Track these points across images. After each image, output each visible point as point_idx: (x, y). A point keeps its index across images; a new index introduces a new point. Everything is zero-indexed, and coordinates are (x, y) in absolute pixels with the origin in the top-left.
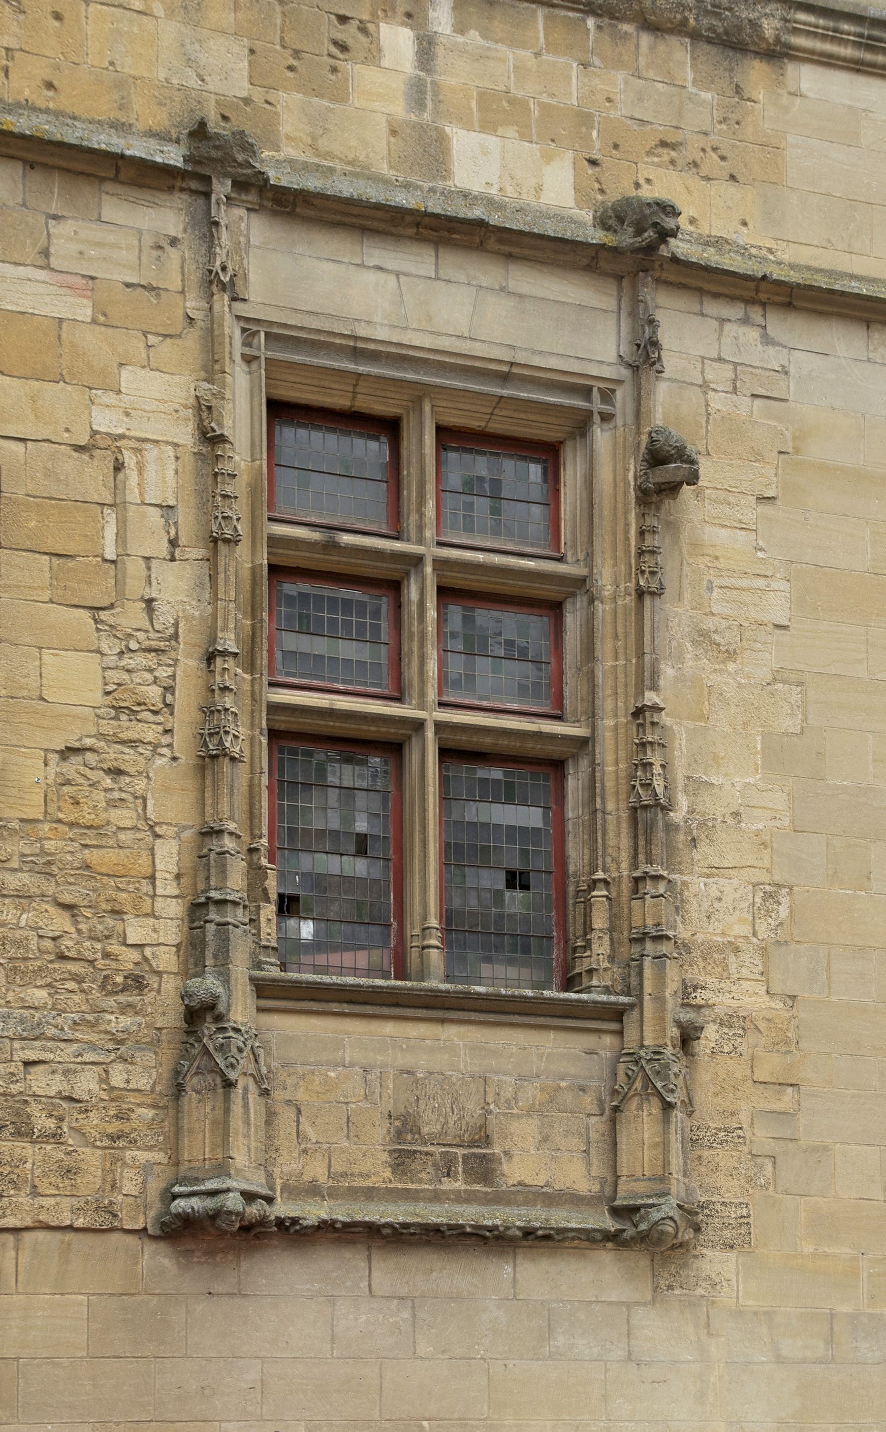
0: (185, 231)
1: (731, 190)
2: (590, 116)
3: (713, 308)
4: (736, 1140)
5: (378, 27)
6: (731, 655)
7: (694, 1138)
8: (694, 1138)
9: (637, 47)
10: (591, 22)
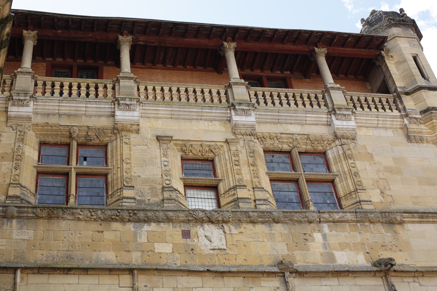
0: (280, 285)
1: (401, 253)
2: (364, 243)
3: (406, 280)
5: (313, 234)
9: (370, 227)
10: (359, 224)
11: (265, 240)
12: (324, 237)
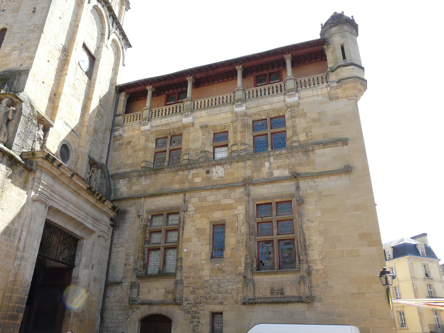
3: (307, 181)
6: (313, 222)
10: (289, 154)
11: (242, 170)
12: (270, 164)
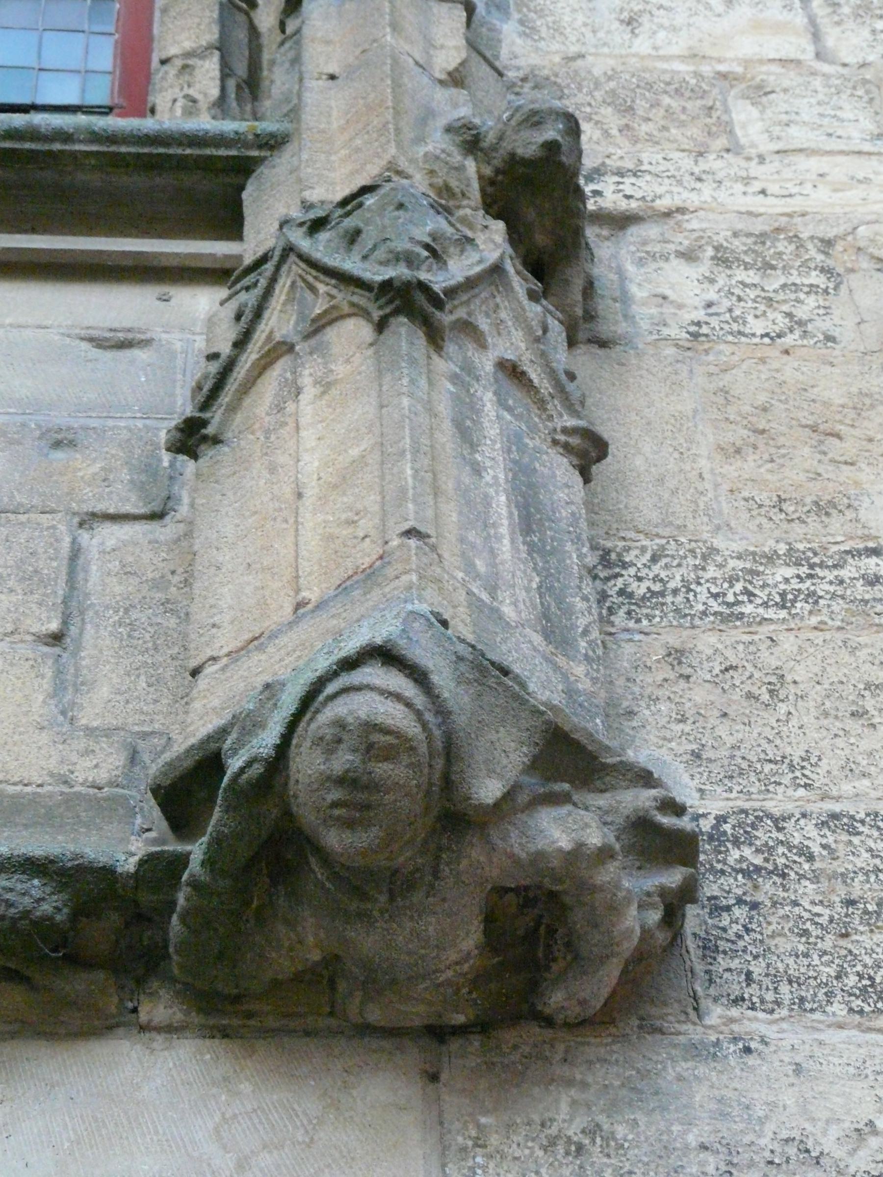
4: (860, 590)
7: (640, 589)
8: (640, 589)
